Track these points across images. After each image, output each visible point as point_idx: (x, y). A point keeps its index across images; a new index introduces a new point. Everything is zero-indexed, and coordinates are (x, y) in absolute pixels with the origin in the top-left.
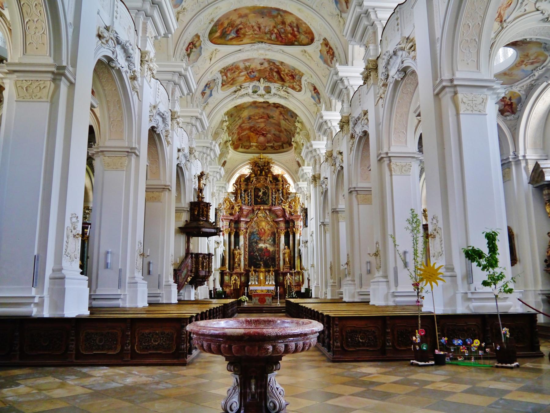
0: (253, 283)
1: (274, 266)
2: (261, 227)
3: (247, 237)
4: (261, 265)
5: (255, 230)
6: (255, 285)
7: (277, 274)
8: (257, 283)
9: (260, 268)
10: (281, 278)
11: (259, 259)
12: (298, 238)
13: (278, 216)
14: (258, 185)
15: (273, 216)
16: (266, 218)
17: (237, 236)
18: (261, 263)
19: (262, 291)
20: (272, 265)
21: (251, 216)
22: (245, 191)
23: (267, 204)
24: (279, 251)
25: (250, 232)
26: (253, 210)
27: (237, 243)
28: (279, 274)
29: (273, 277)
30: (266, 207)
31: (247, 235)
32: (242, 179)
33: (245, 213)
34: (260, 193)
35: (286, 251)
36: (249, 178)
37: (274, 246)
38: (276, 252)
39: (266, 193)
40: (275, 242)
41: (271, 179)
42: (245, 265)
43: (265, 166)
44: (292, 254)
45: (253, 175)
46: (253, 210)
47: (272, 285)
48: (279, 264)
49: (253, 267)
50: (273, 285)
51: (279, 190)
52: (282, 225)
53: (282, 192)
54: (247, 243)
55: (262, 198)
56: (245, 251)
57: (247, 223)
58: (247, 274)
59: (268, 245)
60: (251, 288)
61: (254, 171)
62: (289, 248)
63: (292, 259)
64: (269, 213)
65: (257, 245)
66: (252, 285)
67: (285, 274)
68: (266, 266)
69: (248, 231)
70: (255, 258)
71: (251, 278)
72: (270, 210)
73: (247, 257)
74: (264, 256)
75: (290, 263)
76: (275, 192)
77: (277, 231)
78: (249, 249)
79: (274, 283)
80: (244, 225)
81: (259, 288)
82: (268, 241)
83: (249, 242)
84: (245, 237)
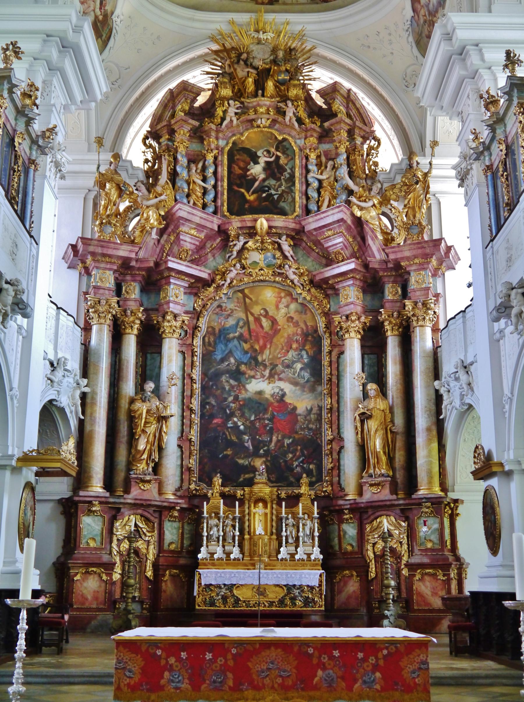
0: (219, 553)
1: (316, 479)
2: (257, 310)
3: (199, 351)
4: (254, 470)
5: (231, 322)
6: (227, 561)
7: (330, 512)
8: (236, 553)
9: (250, 483)
10: (350, 530)
11: (249, 444)
12: (429, 344)
13: (329, 260)
14: (248, 137)
15: (309, 264)
16: (279, 271)
17: (151, 341)
18: (259, 464)
19: (261, 590)
20: (309, 473)
21: (215, 261)
22: (192, 160)
23: (283, 213)
24: (336, 411)
25: (211, 331)
26: (222, 231)
27: (148, 371)
28: (340, 512)
29: (310, 527)
30: (279, 221)
31: (198, 342)
32: (182, 106)
33: (189, 238)
34: (257, 170)
35: (371, 404)
36: (207, 111)
37: (313, 390)
38: (325, 415)
39: (281, 169)
40: (322, 374)
41: (303, 114)
42: (184, 470)
43: (275, 62)
44: (399, 420)
45: (226, 92)
46: (222, 231)
47: (307, 562)
48: (338, 467)
49: (218, 480)
50: (313, 565)
51: (331, 157)
52: (351, 296)
53: (349, 163)
54: (197, 374)
55: (261, 189)
56: (185, 408)
57: (196, 286)
58: (191, 512)
59: (287, 387)
60: (207, 576)
61: (227, 76)
62: (383, 391)
63: (400, 443)
64: (295, 247)
65: (241, 385)
66: (212, 562)
67: (364, 513)
68: (280, 474)
69: (203, 323)
70: (230, 444)
71: (211, 528)
72: (297, 236)
73: (194, 435)
74: (271, 432)
75: (391, 460)
76: (319, 165)
77: (329, 325)
78: (203, 405)
79: (317, 554)
80: (182, 298)
81: (245, 578)
82: (288, 366)
83: (204, 374)
84: (187, 351)
